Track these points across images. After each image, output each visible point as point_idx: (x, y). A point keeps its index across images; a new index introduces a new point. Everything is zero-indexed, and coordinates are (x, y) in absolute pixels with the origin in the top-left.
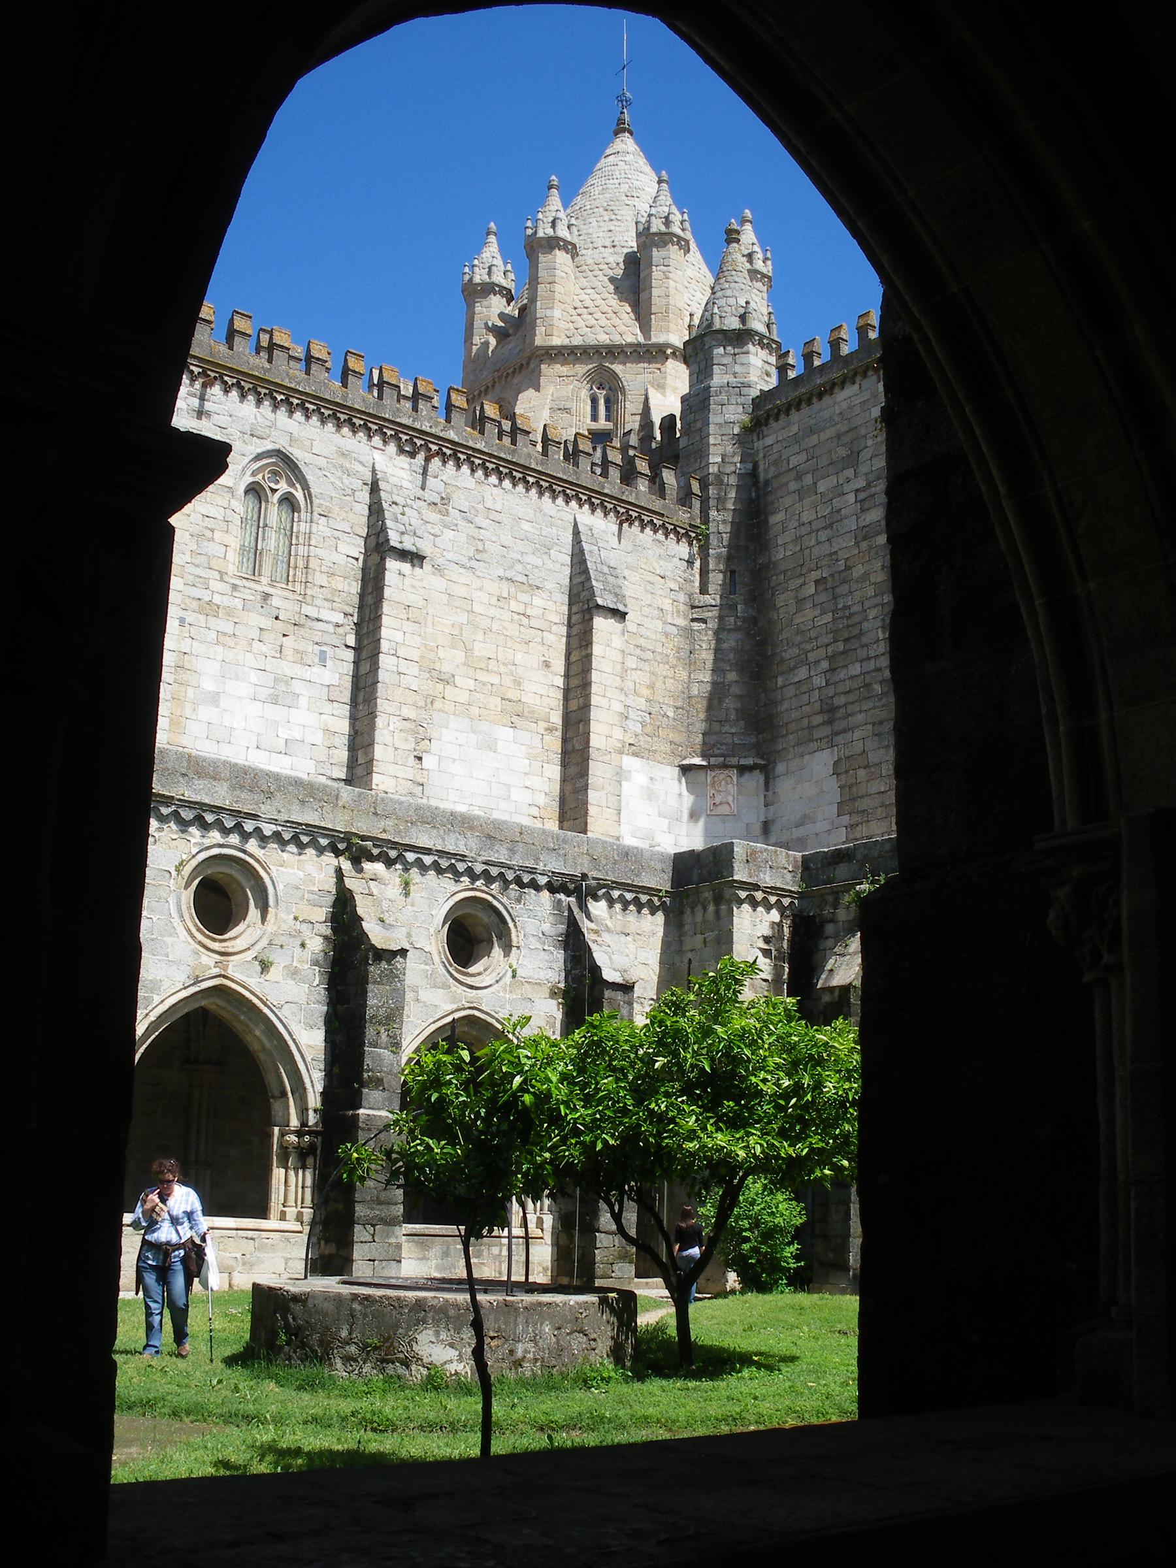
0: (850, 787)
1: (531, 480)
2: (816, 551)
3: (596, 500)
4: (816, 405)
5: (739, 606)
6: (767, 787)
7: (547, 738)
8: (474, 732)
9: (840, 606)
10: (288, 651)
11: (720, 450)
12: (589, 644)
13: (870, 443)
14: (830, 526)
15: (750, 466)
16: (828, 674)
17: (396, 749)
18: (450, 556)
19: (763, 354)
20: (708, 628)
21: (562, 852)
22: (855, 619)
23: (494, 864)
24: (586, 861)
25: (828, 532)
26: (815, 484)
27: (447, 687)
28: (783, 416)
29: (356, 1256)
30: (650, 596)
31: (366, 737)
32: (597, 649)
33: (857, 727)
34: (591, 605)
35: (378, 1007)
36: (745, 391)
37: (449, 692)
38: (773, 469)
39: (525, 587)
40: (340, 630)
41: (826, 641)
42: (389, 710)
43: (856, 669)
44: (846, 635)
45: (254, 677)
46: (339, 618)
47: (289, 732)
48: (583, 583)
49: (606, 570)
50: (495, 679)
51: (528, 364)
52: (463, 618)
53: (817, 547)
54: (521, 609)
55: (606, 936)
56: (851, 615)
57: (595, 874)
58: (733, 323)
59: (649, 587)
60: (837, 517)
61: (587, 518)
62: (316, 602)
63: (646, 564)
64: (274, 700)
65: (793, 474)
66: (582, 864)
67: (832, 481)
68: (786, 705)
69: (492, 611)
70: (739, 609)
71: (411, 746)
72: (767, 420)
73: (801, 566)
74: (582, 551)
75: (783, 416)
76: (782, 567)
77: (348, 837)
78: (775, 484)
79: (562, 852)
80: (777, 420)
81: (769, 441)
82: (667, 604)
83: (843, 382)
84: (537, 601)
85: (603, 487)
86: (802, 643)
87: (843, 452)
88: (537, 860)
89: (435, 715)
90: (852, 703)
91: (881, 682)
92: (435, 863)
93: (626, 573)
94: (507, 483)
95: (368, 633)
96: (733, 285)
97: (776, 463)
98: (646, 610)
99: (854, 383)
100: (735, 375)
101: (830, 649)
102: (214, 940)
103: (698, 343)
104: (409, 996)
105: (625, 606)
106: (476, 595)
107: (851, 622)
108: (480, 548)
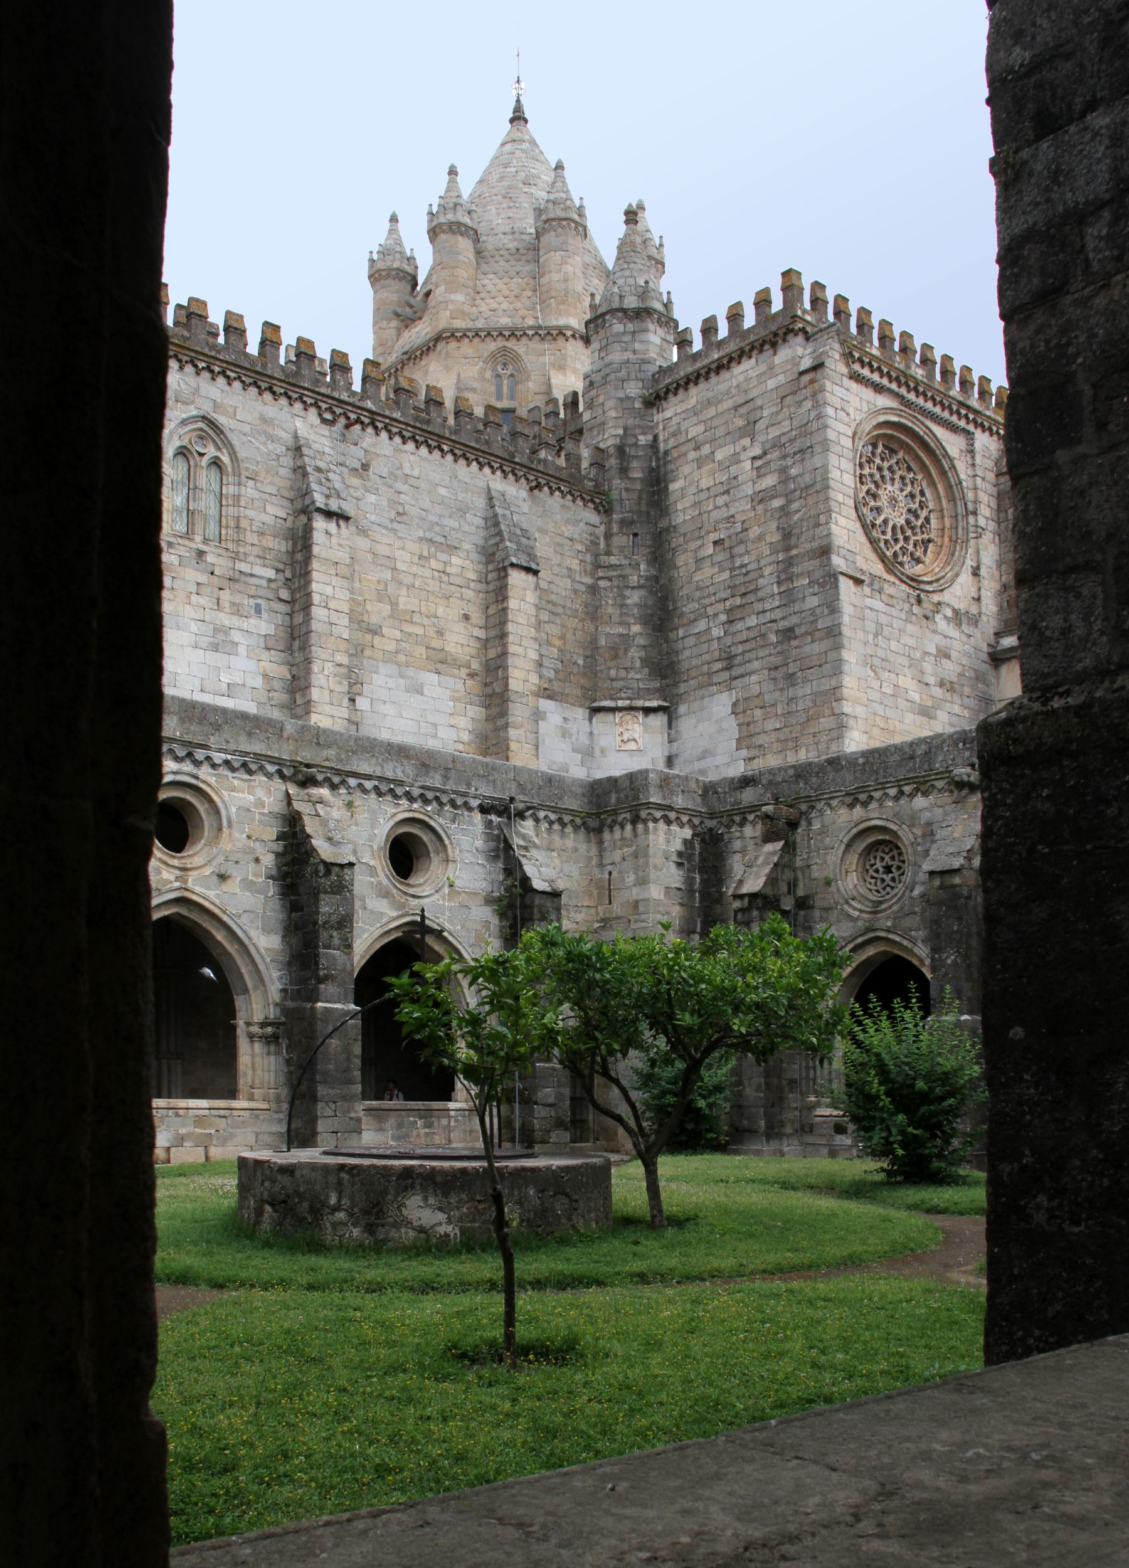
1: (445, 448)
2: (716, 515)
3: (508, 466)
4: (714, 379)
9: (737, 564)
10: (226, 604)
11: (621, 422)
12: (505, 598)
13: (765, 413)
14: (727, 492)
15: (650, 438)
16: (726, 626)
17: (332, 691)
18: (373, 518)
19: (661, 331)
20: (611, 587)
21: (491, 778)
22: (752, 576)
23: (429, 789)
24: (513, 785)
25: (725, 498)
26: (713, 453)
27: (377, 638)
29: (320, 1128)
30: (559, 557)
31: (303, 681)
32: (512, 604)
34: (506, 564)
35: (330, 914)
36: (644, 367)
38: (672, 440)
39: (444, 547)
40: (273, 585)
41: (724, 596)
42: (324, 656)
43: (752, 621)
44: (743, 590)
45: (194, 627)
46: (271, 573)
48: (497, 544)
49: (518, 532)
51: (435, 346)
52: (388, 575)
53: (715, 512)
54: (441, 567)
55: (534, 852)
57: (522, 798)
58: (631, 302)
59: (558, 549)
60: (734, 483)
61: (498, 483)
64: (215, 648)
65: (692, 445)
66: (510, 789)
67: (729, 450)
69: (415, 569)
71: (345, 688)
72: (667, 393)
74: (496, 515)
75: (681, 391)
76: (682, 531)
77: (296, 766)
78: (675, 453)
79: (491, 778)
80: (676, 394)
81: (668, 414)
82: (575, 564)
83: (742, 355)
84: (455, 560)
85: (514, 457)
86: (700, 599)
87: (740, 422)
88: (469, 785)
89: (365, 662)
91: (777, 632)
92: (376, 788)
93: (537, 535)
94: (424, 450)
95: (300, 588)
96: (631, 266)
97: (674, 435)
98: (556, 569)
99: (750, 357)
100: (634, 352)
101: (728, 603)
102: (174, 857)
103: (600, 321)
104: (357, 904)
105: (538, 564)
106: (398, 554)
107: (747, 579)
108: (401, 511)
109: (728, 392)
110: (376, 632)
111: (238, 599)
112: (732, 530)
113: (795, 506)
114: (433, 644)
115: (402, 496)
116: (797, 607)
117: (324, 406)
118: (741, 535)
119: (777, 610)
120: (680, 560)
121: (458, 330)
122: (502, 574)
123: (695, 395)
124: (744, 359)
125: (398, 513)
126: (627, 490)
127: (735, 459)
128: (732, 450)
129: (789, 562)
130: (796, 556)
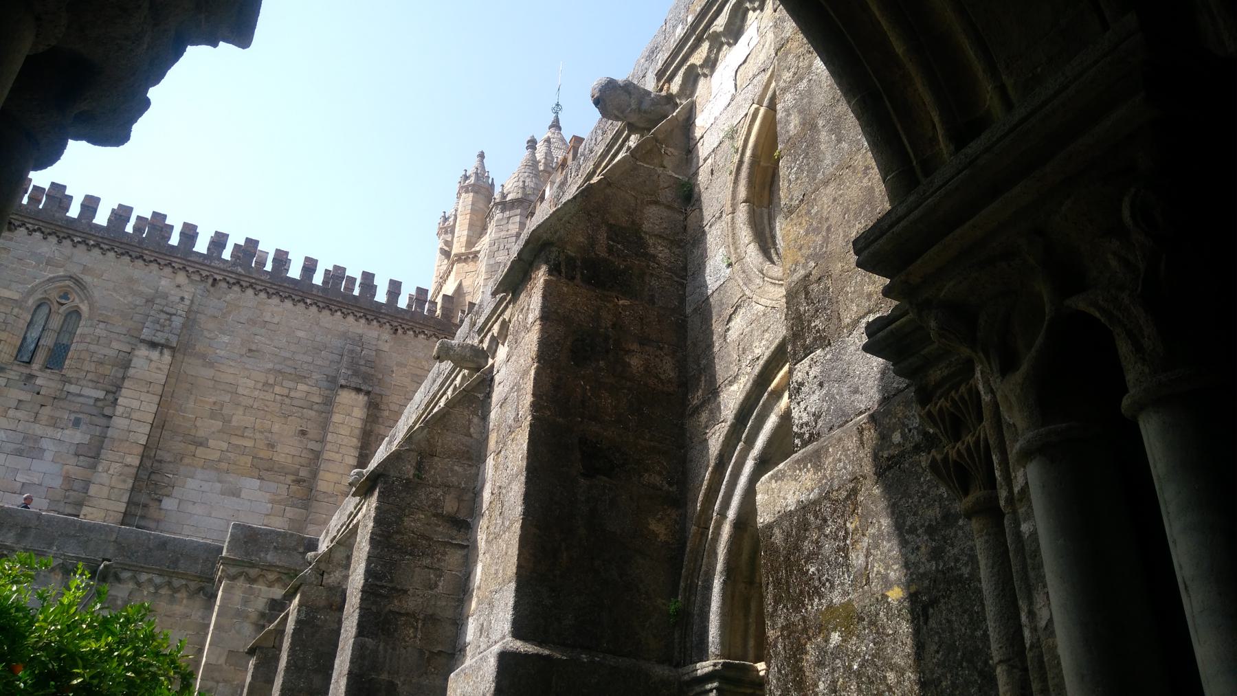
1: (309, 301)
7: (294, 488)
8: (220, 482)
18: (222, 353)
32: (336, 418)
37: (200, 451)
40: (100, 404)
47: (28, 477)
50: (249, 443)
54: (285, 392)
62: (81, 383)
63: (415, 362)
64: (19, 453)
84: (301, 387)
88: (50, 545)
93: (395, 369)
110: (201, 443)
111: (58, 414)
114: (261, 455)
115: (257, 337)
117: (191, 270)
121: (463, 254)
125: (250, 350)
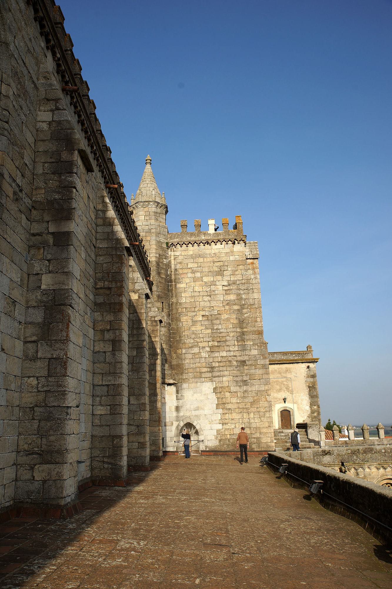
0: (222, 398)
2: (202, 304)
5: (165, 317)
6: (177, 392)
9: (215, 328)
14: (210, 296)
25: (209, 298)
28: (184, 246)
33: (224, 376)
38: (179, 265)
41: (208, 340)
43: (224, 354)
44: (219, 340)
56: (220, 333)
65: (190, 271)
68: (187, 361)
70: (165, 319)
73: (194, 308)
81: (177, 253)
90: (222, 366)
91: (237, 361)
97: (180, 263)
99: (221, 244)
107: (220, 335)
109: (210, 254)
112: (212, 313)
113: (245, 311)
116: (247, 352)
118: (218, 316)
119: (237, 352)
120: (184, 319)
122: (155, 324)
123: (192, 250)
124: (219, 243)
126: (160, 282)
127: (213, 283)
128: (212, 279)
129: (243, 333)
130: (246, 332)
